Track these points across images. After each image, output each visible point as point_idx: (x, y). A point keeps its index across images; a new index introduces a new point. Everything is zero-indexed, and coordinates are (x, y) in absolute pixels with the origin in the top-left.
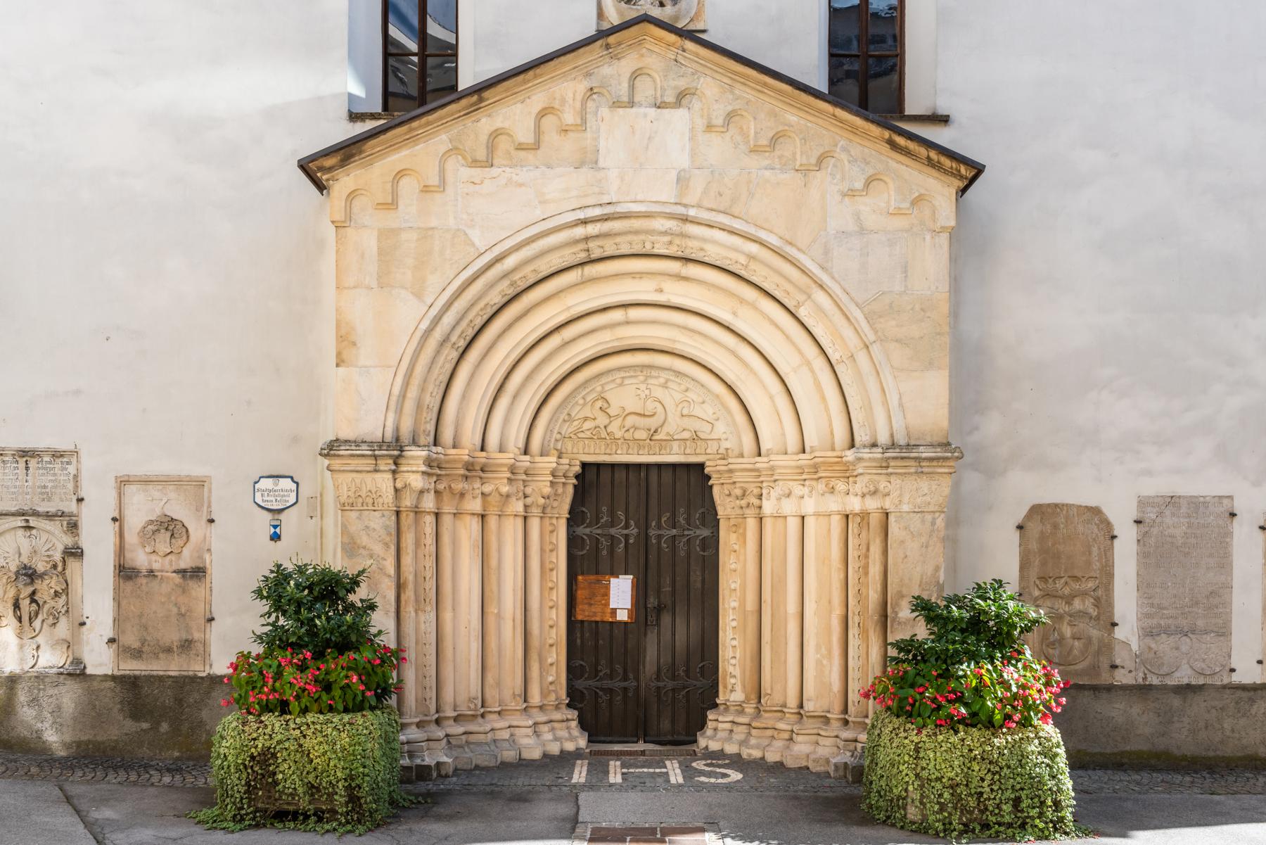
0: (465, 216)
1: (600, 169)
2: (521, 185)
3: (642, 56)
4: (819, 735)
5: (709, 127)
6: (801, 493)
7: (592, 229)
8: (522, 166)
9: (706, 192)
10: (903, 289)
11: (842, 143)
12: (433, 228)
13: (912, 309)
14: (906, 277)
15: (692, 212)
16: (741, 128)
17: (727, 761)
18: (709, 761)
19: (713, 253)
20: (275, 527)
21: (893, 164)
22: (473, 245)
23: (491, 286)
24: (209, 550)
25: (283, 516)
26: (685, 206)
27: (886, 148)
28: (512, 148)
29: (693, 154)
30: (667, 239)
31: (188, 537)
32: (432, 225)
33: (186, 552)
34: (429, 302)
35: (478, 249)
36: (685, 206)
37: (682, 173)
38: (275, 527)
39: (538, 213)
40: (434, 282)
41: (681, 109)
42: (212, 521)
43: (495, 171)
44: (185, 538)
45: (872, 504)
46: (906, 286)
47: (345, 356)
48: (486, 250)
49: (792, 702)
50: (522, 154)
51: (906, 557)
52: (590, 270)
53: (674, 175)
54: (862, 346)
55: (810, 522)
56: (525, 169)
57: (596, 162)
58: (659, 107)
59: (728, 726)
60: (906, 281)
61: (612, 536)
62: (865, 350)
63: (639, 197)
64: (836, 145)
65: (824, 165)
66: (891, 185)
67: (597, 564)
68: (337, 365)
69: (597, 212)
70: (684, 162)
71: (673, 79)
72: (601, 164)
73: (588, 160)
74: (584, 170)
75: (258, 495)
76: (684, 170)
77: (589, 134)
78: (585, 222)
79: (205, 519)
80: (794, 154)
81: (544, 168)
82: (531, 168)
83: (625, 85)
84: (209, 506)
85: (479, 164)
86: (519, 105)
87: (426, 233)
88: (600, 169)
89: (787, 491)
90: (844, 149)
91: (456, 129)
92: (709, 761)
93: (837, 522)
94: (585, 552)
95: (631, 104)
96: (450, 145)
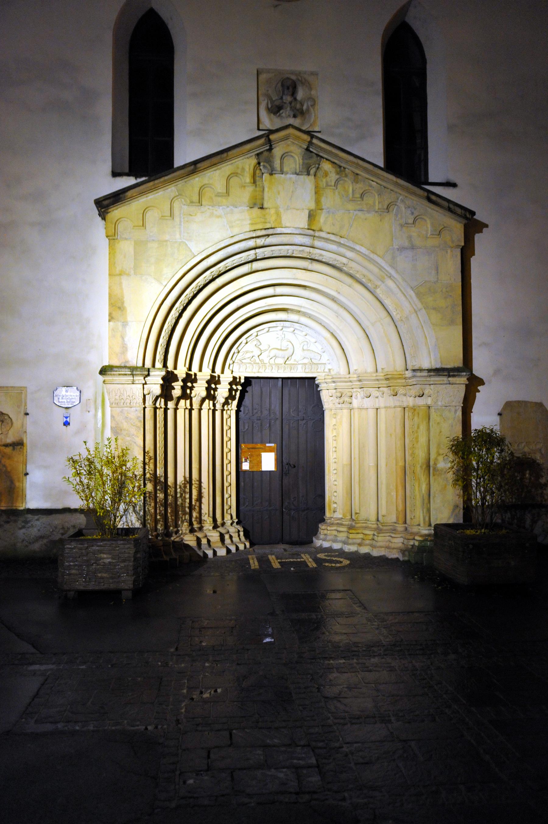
3: (288, 145)
4: (391, 536)
6: (377, 395)
8: (219, 206)
10: (436, 280)
11: (400, 198)
12: (166, 241)
13: (441, 291)
14: (438, 273)
15: (317, 234)
16: (345, 188)
17: (337, 554)
18: (326, 554)
19: (327, 256)
20: (66, 418)
21: (429, 210)
22: (191, 251)
24: (26, 432)
25: (70, 411)
27: (426, 203)
31: (12, 424)
32: (167, 239)
33: (11, 432)
34: (165, 284)
35: (193, 253)
36: (313, 230)
37: (312, 212)
38: (66, 418)
41: (310, 177)
42: (27, 414)
43: (203, 209)
44: (10, 424)
45: (421, 402)
46: (438, 278)
47: (114, 314)
48: (198, 254)
50: (219, 199)
51: (441, 432)
52: (256, 265)
54: (413, 311)
55: (382, 412)
56: (221, 208)
58: (298, 174)
59: (335, 533)
60: (437, 275)
62: (415, 314)
63: (288, 225)
64: (398, 199)
65: (391, 209)
66: (428, 221)
68: (109, 321)
69: (264, 232)
72: (265, 206)
75: (56, 398)
76: (312, 210)
79: (23, 413)
80: (374, 203)
81: (232, 207)
82: (225, 207)
84: (26, 405)
85: (194, 204)
89: (369, 395)
90: (402, 201)
91: (181, 183)
92: (326, 554)
95: (282, 172)
96: (177, 193)
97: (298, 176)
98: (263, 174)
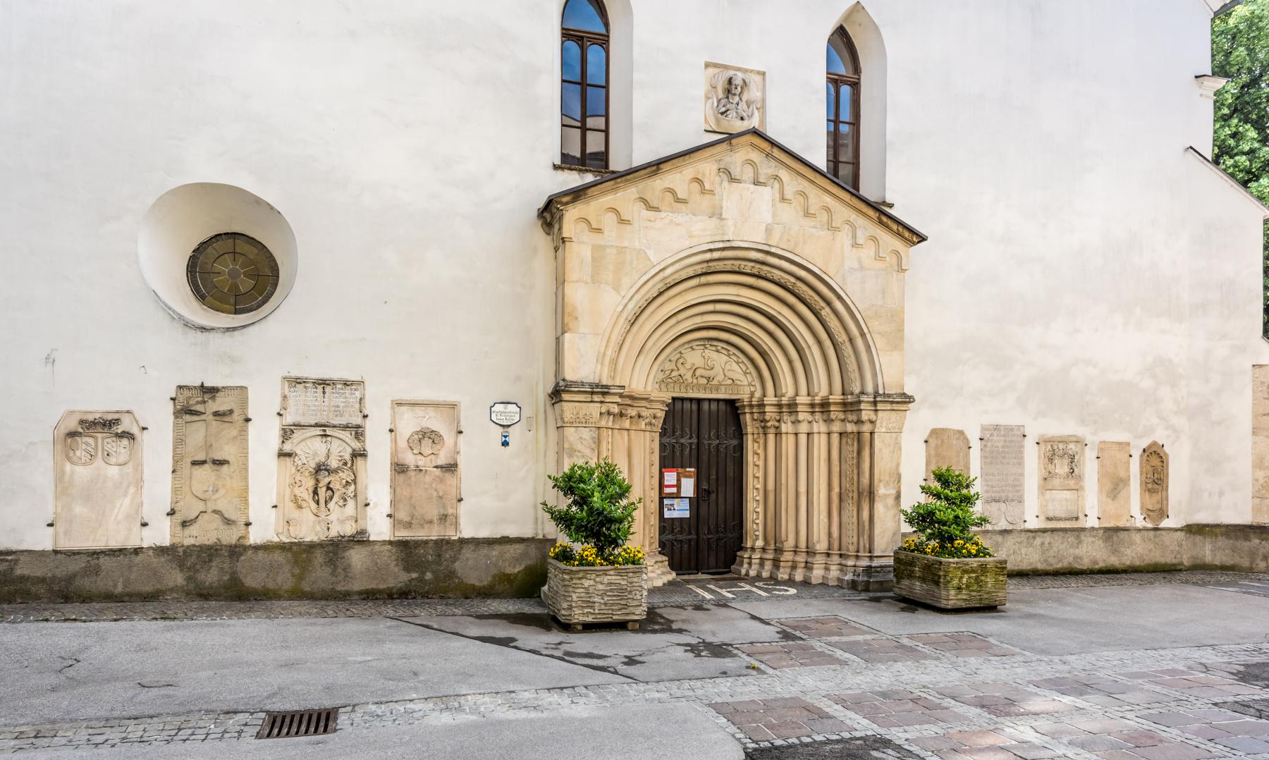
0: (645, 241)
1: (722, 219)
2: (678, 225)
3: (748, 152)
5: (783, 199)
7: (716, 255)
9: (781, 238)
23: (654, 286)
26: (769, 245)
28: (672, 201)
29: (774, 215)
30: (752, 264)
32: (625, 245)
39: (687, 243)
40: (626, 281)
49: (803, 545)
53: (764, 226)
57: (721, 215)
61: (682, 444)
67: (673, 461)
70: (768, 219)
71: (765, 169)
72: (724, 217)
73: (717, 214)
74: (714, 219)
76: (769, 224)
77: (717, 197)
78: (711, 250)
83: (739, 169)
86: (678, 174)
87: (621, 250)
88: (722, 219)
93: (835, 438)
94: (666, 454)
97: (756, 187)
98: (722, 181)
